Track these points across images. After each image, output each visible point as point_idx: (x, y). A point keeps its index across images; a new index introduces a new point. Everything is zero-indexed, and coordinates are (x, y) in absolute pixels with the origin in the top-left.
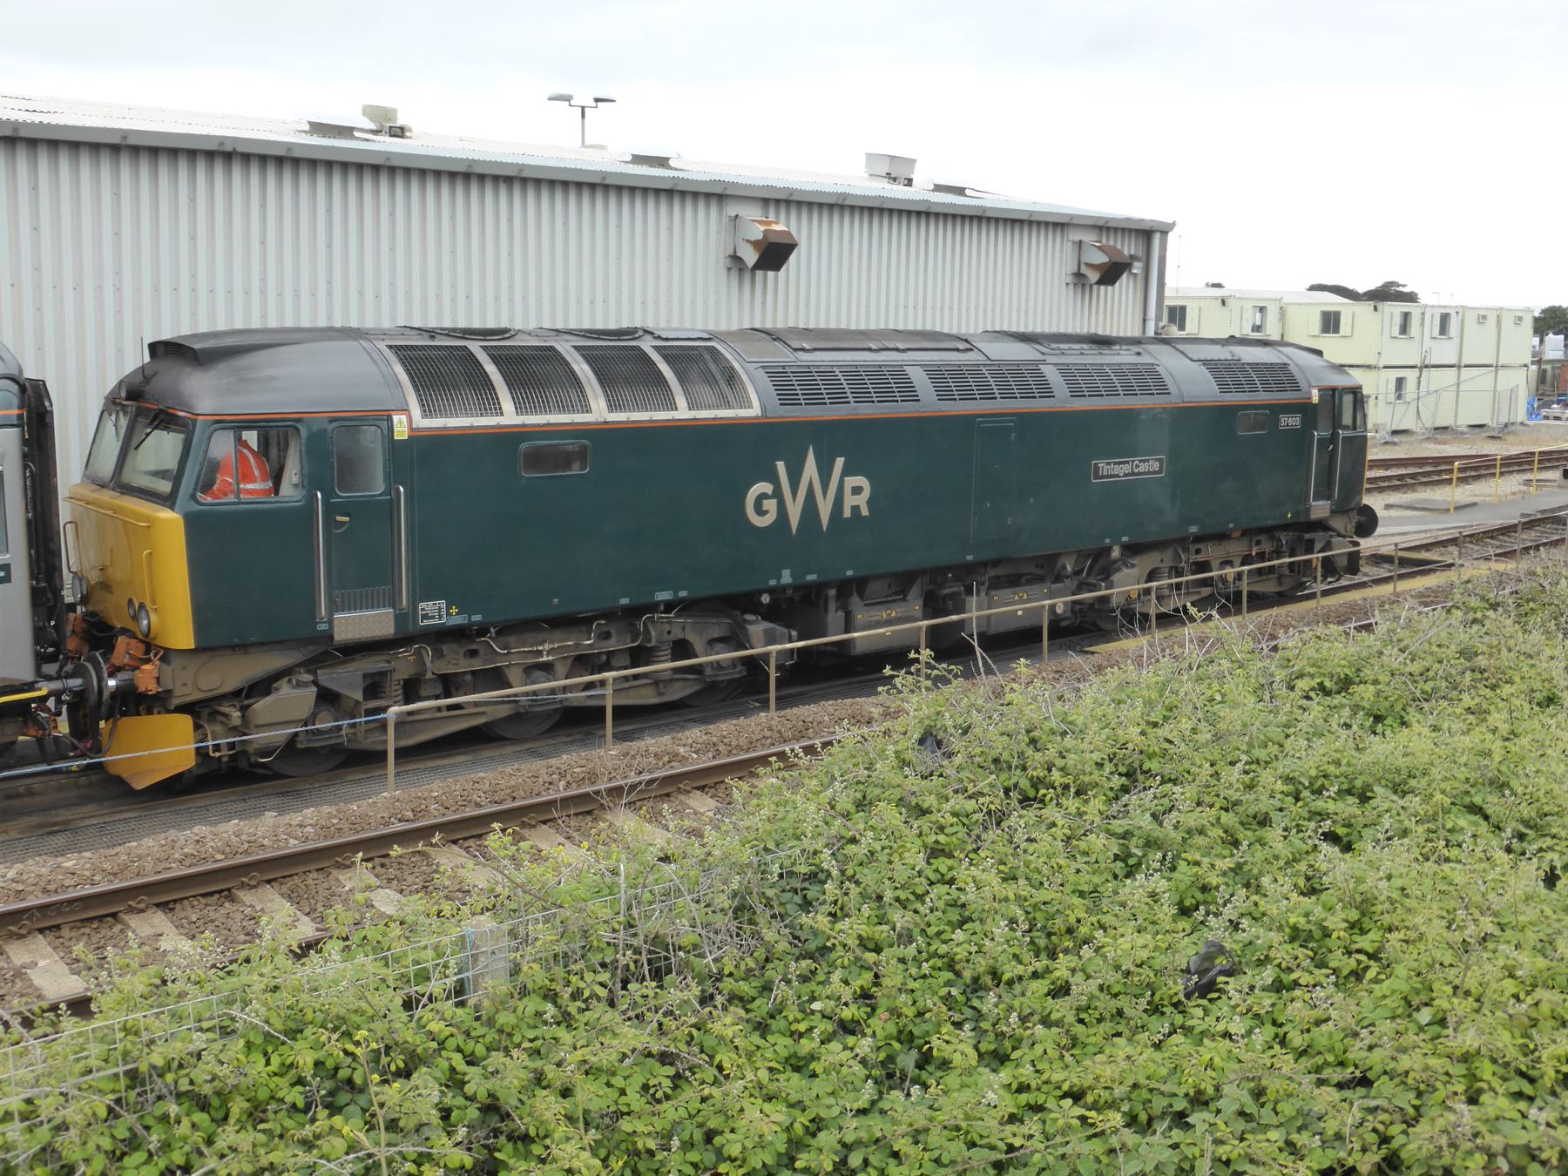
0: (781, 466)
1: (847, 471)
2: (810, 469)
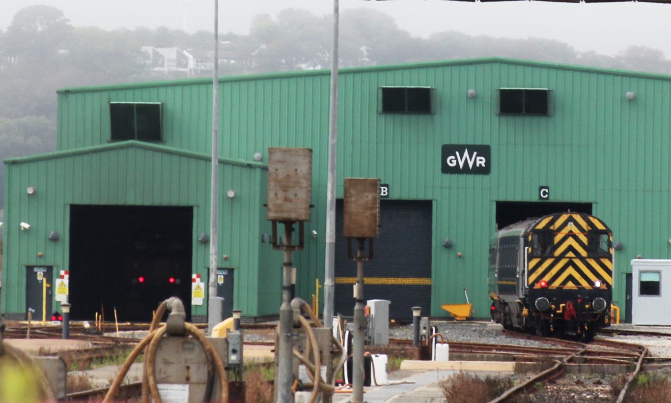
0: (457, 153)
2: (466, 154)
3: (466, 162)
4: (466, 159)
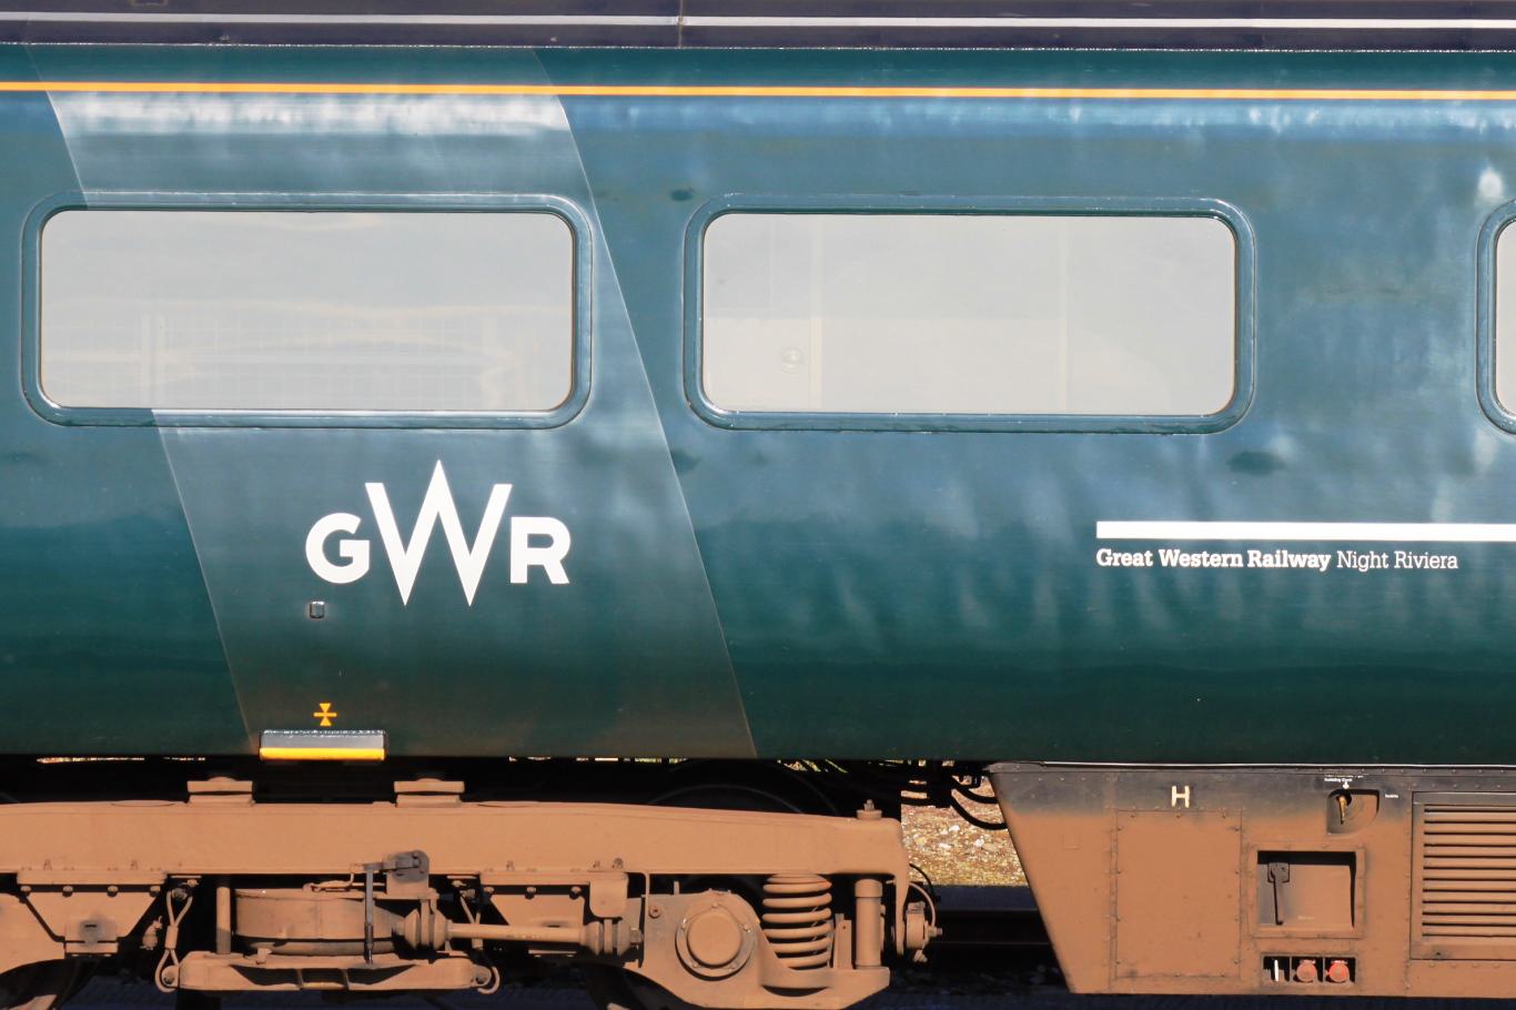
0: (377, 493)
1: (523, 504)
2: (439, 500)
3: (438, 560)
4: (438, 534)
